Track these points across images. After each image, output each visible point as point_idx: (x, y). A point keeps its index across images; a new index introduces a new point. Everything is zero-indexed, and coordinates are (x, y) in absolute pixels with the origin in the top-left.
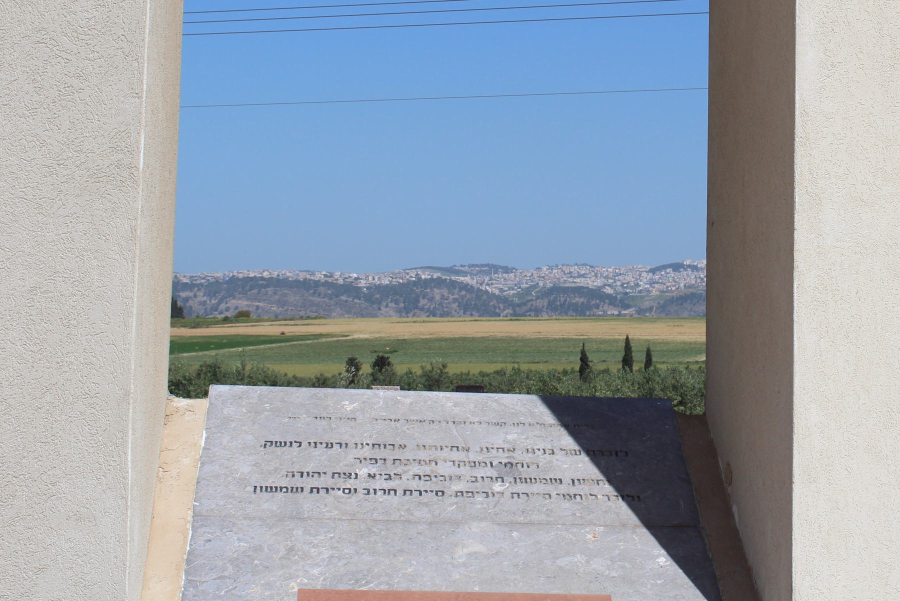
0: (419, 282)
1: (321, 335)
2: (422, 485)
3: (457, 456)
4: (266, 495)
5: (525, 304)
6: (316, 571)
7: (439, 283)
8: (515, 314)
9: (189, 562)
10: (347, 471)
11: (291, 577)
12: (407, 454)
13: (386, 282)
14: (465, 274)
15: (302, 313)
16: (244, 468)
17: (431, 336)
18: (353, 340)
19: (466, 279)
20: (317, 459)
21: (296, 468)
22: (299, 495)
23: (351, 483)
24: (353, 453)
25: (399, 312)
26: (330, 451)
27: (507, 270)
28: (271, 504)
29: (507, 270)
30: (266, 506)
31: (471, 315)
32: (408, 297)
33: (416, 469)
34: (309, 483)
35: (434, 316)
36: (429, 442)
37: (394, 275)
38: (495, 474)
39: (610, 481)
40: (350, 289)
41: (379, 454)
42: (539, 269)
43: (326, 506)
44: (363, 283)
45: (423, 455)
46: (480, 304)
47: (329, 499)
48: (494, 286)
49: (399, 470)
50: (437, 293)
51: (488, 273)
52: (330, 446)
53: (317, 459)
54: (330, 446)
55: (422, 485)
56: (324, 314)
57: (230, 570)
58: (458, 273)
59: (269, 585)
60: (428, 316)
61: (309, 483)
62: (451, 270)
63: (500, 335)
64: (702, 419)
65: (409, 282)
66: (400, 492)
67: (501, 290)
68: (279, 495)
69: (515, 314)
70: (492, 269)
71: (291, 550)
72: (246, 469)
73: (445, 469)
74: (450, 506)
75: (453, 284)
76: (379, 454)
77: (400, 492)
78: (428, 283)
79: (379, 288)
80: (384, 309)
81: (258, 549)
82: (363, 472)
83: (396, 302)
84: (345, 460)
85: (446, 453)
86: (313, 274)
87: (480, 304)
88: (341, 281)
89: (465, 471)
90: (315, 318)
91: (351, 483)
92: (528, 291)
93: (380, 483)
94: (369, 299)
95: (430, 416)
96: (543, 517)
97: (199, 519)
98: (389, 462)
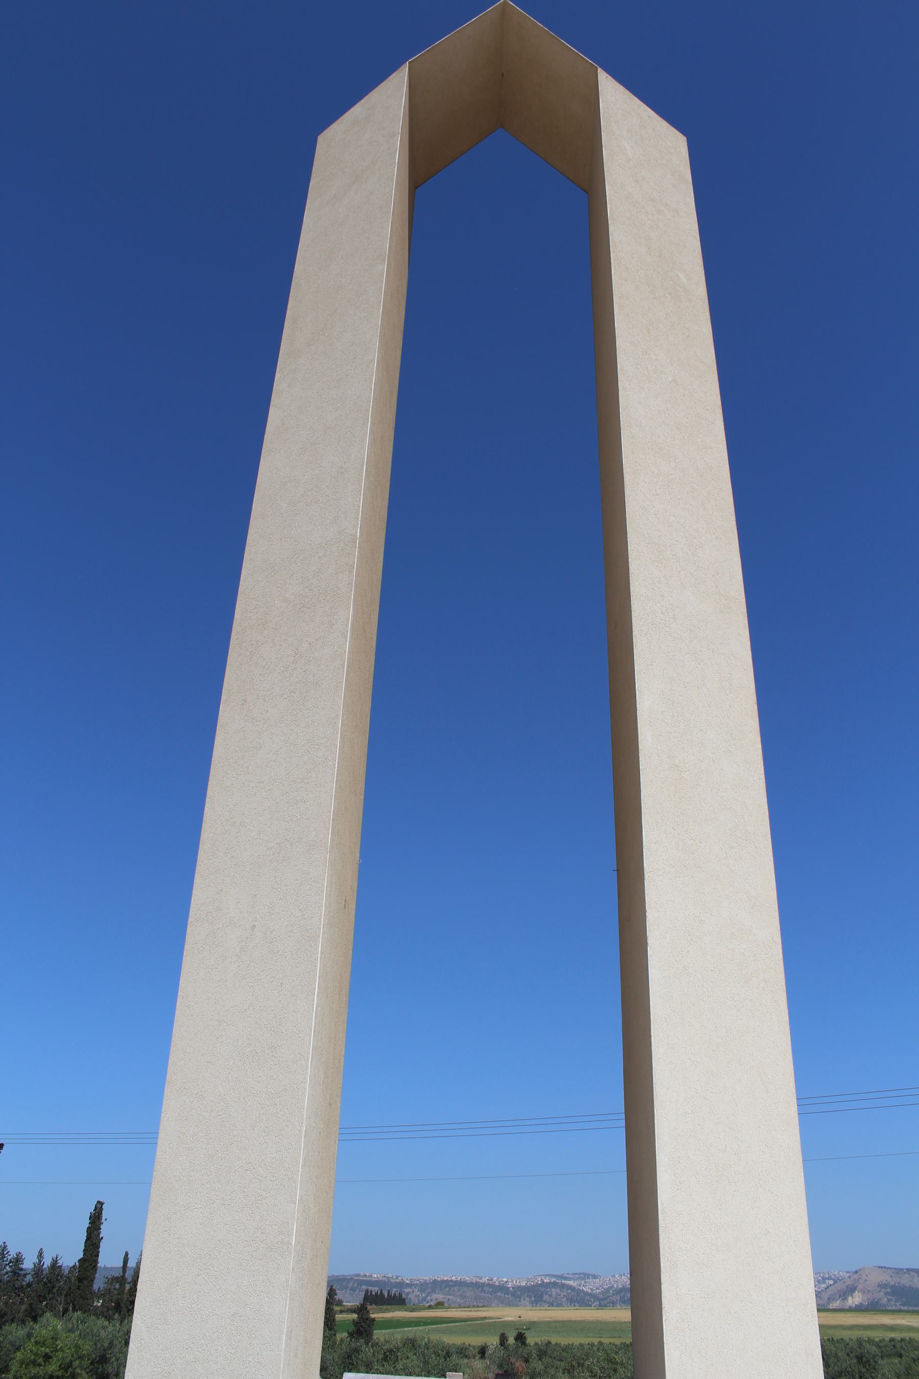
0: (543, 1284)
1: (485, 1318)
5: (606, 1299)
7: (555, 1284)
8: (600, 1305)
13: (523, 1284)
14: (569, 1279)
15: (475, 1303)
18: (504, 1322)
19: (571, 1283)
25: (532, 1303)
27: (595, 1277)
29: (595, 1277)
32: (536, 1294)
37: (528, 1280)
40: (502, 1288)
42: (614, 1276)
44: (510, 1285)
46: (579, 1299)
48: (587, 1287)
50: (554, 1291)
51: (584, 1279)
56: (487, 1305)
58: (566, 1278)
62: (562, 1277)
63: (591, 1319)
65: (537, 1285)
67: (592, 1290)
69: (600, 1305)
70: (586, 1276)
75: (563, 1285)
78: (548, 1285)
79: (519, 1288)
80: (523, 1302)
83: (530, 1297)
86: (481, 1278)
87: (579, 1299)
88: (497, 1283)
92: (607, 1290)
94: (514, 1294)
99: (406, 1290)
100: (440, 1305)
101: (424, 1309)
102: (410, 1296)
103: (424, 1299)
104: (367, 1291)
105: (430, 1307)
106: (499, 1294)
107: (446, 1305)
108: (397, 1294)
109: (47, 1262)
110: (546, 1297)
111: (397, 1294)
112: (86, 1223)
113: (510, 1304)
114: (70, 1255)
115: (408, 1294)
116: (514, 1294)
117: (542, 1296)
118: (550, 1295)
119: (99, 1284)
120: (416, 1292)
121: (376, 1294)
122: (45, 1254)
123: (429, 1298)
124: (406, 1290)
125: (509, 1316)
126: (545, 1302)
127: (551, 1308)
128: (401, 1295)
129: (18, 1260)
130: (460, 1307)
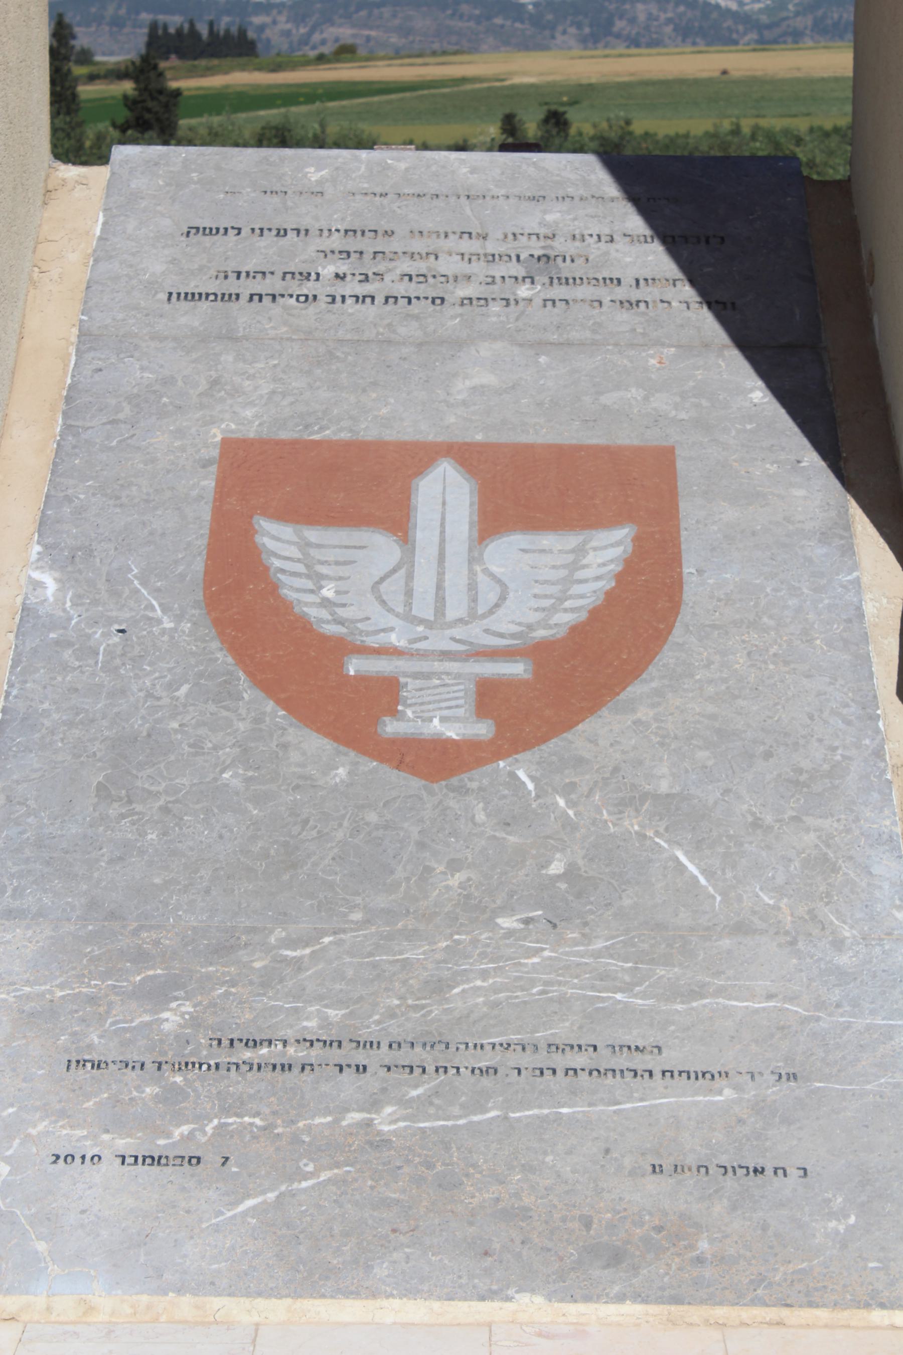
1: (464, 80)
2: (413, 289)
3: (466, 246)
4: (184, 305)
6: (249, 413)
9: (68, 399)
10: (305, 269)
11: (213, 422)
12: (395, 245)
15: (436, 46)
16: (155, 266)
17: (632, 78)
20: (263, 253)
21: (231, 266)
22: (234, 306)
23: (308, 288)
24: (316, 243)
26: (283, 242)
28: (192, 317)
30: (183, 320)
31: (694, 44)
33: (406, 266)
34: (247, 287)
35: (638, 45)
36: (428, 225)
38: (521, 272)
39: (692, 282)
41: (352, 244)
43: (270, 320)
45: (418, 245)
47: (276, 310)
49: (381, 268)
52: (282, 233)
53: (263, 253)
54: (282, 233)
55: (413, 289)
57: (127, 411)
59: (180, 433)
60: (628, 47)
61: (247, 287)
64: (843, 190)
66: (379, 299)
68: (204, 305)
71: (215, 383)
72: (159, 268)
73: (448, 265)
74: (450, 320)
76: (352, 244)
77: (379, 299)
81: (168, 381)
82: (328, 270)
83: (579, 26)
84: (304, 254)
85: (452, 243)
89: (478, 268)
90: (455, 53)
91: (308, 288)
93: (352, 287)
95: (433, 187)
96: (588, 334)
97: (88, 339)
98: (367, 257)
99: (257, 20)
100: (345, 52)
101: (306, 63)
102: (268, 33)
103: (305, 41)
104: (154, 26)
105: (321, 59)
106: (498, 21)
107: (362, 52)
108: (234, 30)
110: (619, 25)
111: (234, 30)
113: (527, 45)
115: (261, 28)
116: (536, 21)
117: (610, 23)
118: (633, 21)
120: (284, 24)
121: (179, 32)
123: (316, 37)
124: (257, 20)
125: (524, 73)
126: (618, 36)
127: (634, 51)
128: (242, 33)
130: (398, 54)
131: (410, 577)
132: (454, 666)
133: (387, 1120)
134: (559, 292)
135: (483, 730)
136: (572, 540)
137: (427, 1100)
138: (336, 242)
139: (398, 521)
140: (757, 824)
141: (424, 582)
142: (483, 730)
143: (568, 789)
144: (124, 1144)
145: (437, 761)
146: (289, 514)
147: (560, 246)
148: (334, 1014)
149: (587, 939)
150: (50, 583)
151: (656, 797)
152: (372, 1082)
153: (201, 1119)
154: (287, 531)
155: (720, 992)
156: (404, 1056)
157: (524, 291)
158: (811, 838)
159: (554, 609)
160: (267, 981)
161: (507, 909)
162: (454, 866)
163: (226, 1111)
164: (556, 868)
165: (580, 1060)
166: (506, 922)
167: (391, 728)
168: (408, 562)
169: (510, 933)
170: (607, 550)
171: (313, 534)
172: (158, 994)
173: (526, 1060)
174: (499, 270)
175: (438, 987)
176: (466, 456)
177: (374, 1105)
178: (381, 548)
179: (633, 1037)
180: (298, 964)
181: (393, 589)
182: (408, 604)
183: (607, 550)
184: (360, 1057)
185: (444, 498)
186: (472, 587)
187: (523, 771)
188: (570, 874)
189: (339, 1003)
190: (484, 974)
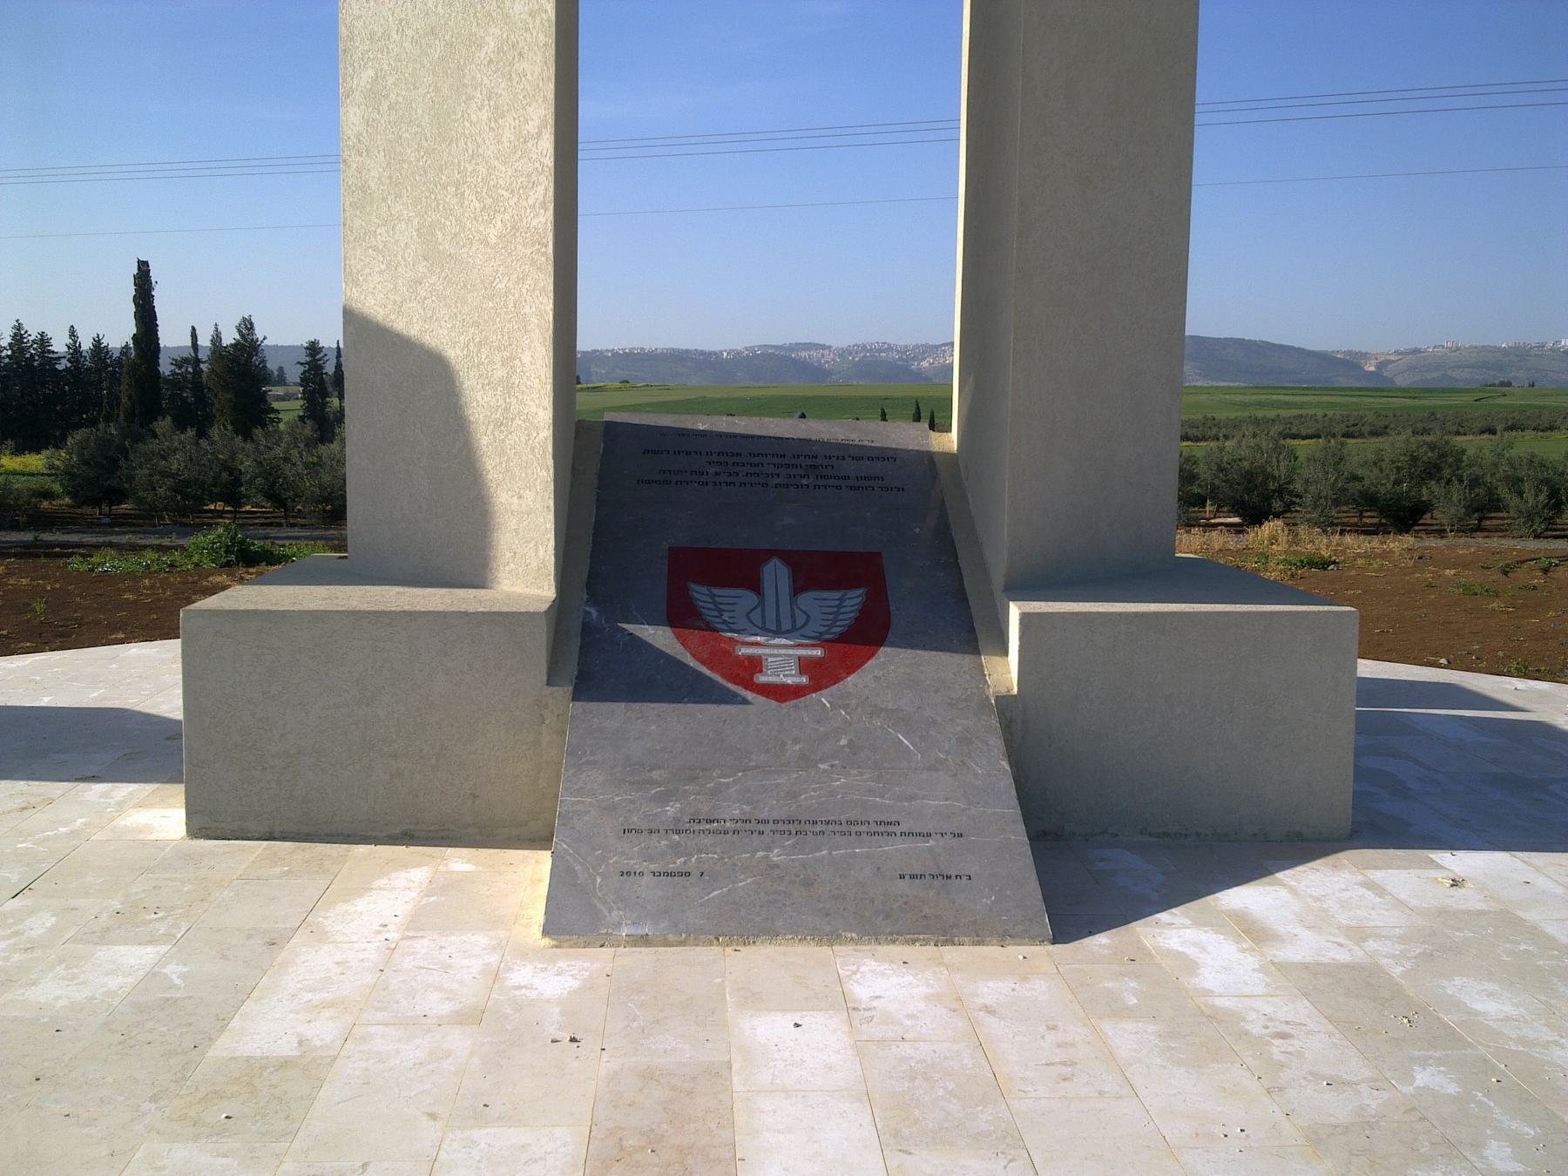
3: (777, 460)
23: (703, 478)
33: (748, 469)
54: (688, 453)
82: (712, 470)
91: (703, 478)
93: (724, 478)
109: (86, 345)
112: (131, 290)
114: (119, 332)
119: (165, 367)
122: (79, 333)
129: (43, 341)
131: (763, 610)
132: (791, 652)
133: (776, 856)
134: (821, 482)
135: (804, 680)
136: (837, 594)
137: (794, 846)
138: (715, 458)
139: (756, 587)
140: (934, 722)
141: (771, 614)
142: (804, 680)
143: (846, 707)
144: (653, 867)
145: (780, 693)
146: (700, 582)
147: (819, 461)
148: (747, 808)
149: (861, 774)
150: (594, 612)
151: (886, 710)
152: (766, 838)
153: (690, 855)
154: (703, 589)
155: (924, 797)
156: (781, 827)
157: (805, 482)
158: (959, 729)
159: (831, 626)
160: (715, 792)
161: (822, 760)
162: (796, 741)
163: (700, 851)
164: (843, 742)
165: (863, 828)
166: (822, 766)
167: (761, 679)
168: (761, 603)
169: (825, 771)
170: (854, 599)
171: (716, 591)
172: (663, 798)
173: (837, 828)
174: (793, 472)
175: (794, 795)
176: (787, 557)
177: (769, 849)
178: (747, 598)
179: (885, 818)
180: (728, 785)
181: (756, 616)
182: (764, 623)
183: (854, 599)
184: (761, 827)
185: (776, 575)
186: (793, 616)
187: (824, 698)
188: (850, 744)
189: (748, 803)
190: (815, 790)
